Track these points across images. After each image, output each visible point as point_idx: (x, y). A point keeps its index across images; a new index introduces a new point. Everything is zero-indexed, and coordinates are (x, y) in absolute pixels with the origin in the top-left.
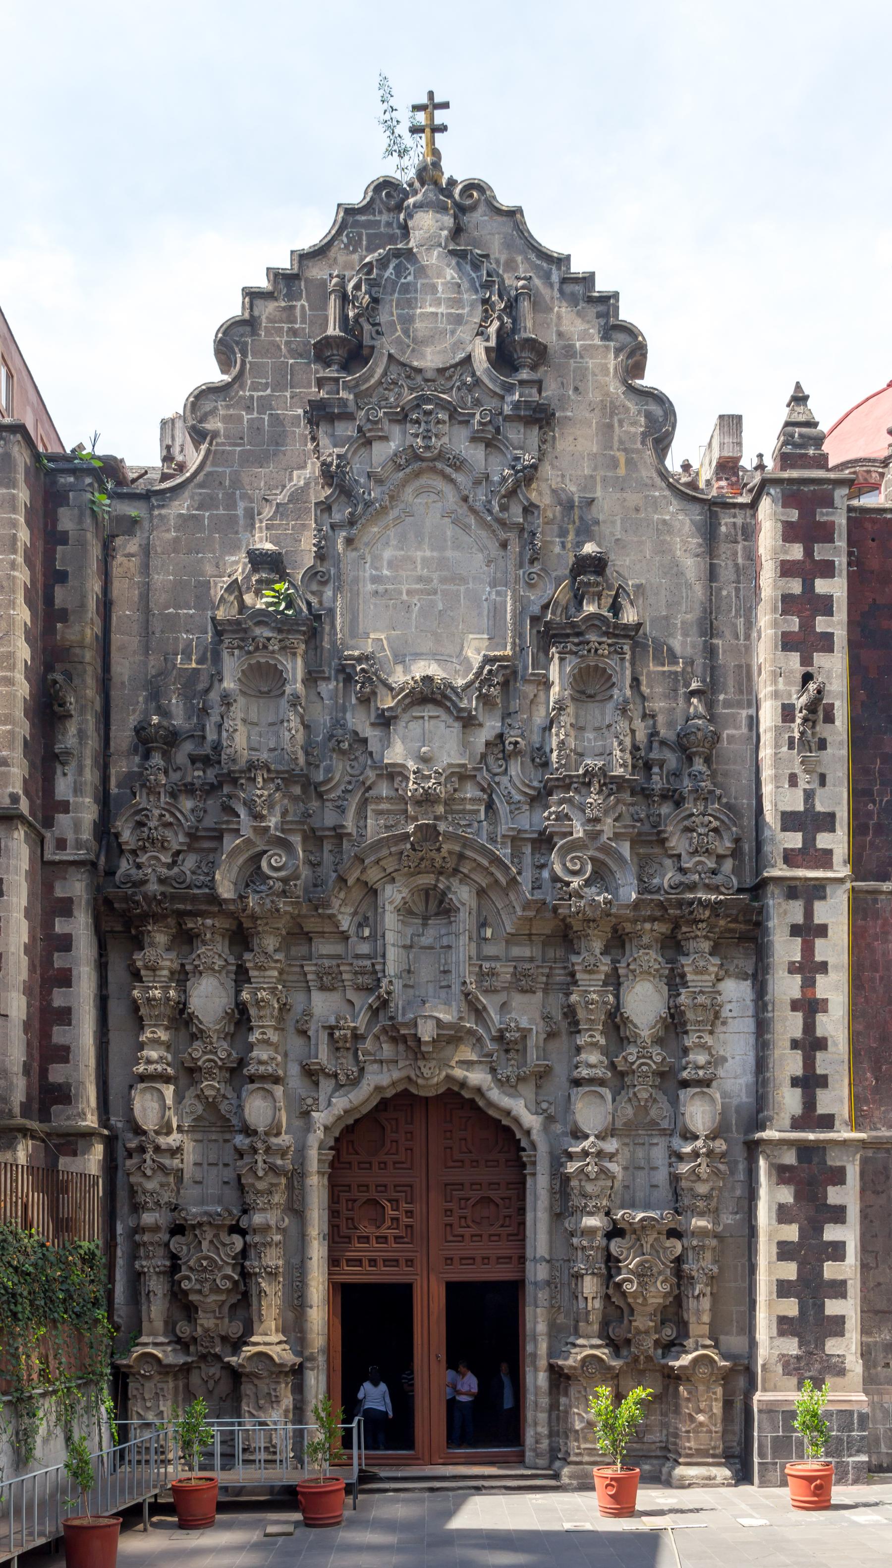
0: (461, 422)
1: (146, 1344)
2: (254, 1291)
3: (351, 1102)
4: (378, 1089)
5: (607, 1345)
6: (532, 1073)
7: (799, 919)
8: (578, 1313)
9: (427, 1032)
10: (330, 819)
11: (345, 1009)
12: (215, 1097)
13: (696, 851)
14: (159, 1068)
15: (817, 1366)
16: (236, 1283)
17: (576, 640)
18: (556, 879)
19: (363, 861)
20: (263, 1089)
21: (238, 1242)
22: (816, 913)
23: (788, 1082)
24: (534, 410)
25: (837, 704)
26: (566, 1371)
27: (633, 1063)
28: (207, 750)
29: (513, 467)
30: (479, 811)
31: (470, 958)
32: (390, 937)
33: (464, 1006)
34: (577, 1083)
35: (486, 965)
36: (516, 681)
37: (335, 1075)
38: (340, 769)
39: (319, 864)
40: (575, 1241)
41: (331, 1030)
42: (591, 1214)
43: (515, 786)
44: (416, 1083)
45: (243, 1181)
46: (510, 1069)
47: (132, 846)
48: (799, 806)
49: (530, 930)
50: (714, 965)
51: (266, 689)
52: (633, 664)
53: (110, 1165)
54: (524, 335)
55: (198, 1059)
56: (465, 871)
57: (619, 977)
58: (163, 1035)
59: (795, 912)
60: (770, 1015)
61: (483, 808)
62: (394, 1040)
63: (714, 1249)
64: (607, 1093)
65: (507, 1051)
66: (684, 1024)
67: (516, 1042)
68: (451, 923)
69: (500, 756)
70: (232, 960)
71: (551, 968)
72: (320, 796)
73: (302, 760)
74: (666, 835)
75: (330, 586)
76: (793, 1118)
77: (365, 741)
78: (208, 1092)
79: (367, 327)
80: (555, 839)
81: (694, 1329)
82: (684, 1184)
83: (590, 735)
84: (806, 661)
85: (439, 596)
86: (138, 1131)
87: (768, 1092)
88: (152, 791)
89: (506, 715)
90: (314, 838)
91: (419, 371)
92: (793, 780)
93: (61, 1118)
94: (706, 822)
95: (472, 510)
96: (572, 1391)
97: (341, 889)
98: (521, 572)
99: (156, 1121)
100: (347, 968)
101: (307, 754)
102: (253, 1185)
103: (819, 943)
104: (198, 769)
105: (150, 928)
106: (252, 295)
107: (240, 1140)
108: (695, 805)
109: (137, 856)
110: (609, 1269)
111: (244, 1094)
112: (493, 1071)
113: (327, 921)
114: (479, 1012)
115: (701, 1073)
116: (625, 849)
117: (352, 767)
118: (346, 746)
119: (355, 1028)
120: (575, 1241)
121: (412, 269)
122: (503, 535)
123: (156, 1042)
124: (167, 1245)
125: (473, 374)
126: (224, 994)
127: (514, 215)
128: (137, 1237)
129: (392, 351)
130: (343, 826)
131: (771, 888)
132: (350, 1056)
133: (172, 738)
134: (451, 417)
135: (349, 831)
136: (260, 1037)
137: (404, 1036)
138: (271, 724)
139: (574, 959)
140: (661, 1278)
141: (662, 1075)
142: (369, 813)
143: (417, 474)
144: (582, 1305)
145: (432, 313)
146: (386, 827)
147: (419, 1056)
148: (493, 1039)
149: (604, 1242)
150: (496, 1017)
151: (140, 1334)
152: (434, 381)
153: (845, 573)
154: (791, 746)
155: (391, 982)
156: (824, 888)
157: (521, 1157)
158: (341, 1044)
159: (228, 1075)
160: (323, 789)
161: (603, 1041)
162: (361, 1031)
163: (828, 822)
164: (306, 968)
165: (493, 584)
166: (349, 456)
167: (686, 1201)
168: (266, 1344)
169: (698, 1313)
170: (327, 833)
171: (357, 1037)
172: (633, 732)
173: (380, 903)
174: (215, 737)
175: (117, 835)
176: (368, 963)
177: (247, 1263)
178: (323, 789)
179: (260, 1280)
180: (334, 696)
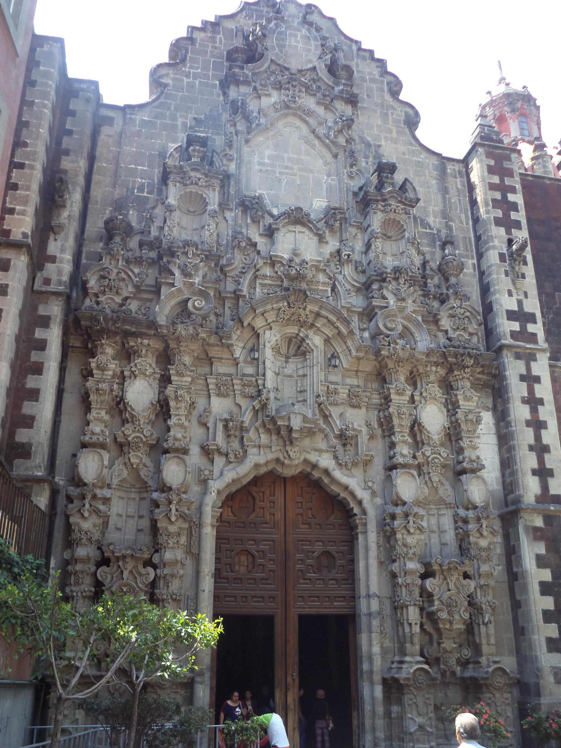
0: (311, 95)
3: (237, 473)
4: (257, 466)
7: (524, 372)
8: (404, 637)
9: (296, 423)
11: (235, 410)
13: (458, 328)
17: (383, 204)
20: (178, 457)
22: (532, 369)
23: (530, 472)
26: (402, 682)
27: (429, 457)
28: (152, 239)
30: (327, 291)
32: (268, 364)
33: (317, 412)
35: (332, 387)
37: (227, 455)
38: (238, 259)
41: (226, 422)
42: (411, 559)
44: (283, 464)
45: (159, 525)
46: (347, 457)
47: (95, 291)
48: (516, 308)
49: (358, 367)
50: (475, 396)
51: (193, 210)
55: (129, 436)
56: (319, 325)
59: (519, 367)
60: (514, 429)
61: (329, 289)
62: (269, 431)
64: (415, 473)
65: (344, 445)
68: (306, 360)
69: (338, 263)
74: (439, 317)
75: (234, 162)
76: (536, 496)
77: (255, 245)
78: (133, 460)
79: (259, 46)
80: (376, 310)
81: (485, 649)
84: (508, 232)
85: (297, 177)
87: (517, 479)
91: (287, 69)
92: (510, 294)
94: (462, 312)
95: (318, 137)
96: (407, 698)
97: (238, 329)
99: (94, 476)
100: (238, 382)
102: (166, 528)
103: (536, 386)
104: (145, 250)
105: (103, 341)
108: (455, 303)
109: (98, 297)
111: (163, 461)
112: (336, 457)
113: (226, 350)
114: (326, 417)
115: (475, 464)
117: (246, 259)
123: (100, 420)
124: (95, 575)
125: (317, 74)
126: (151, 392)
129: (273, 58)
130: (241, 290)
131: (505, 352)
133: (129, 231)
135: (244, 294)
136: (177, 422)
137: (279, 426)
141: (444, 466)
142: (258, 285)
143: (286, 116)
144: (407, 630)
145: (295, 46)
146: (268, 294)
147: (287, 443)
150: (338, 422)
154: (507, 274)
158: (232, 432)
160: (227, 269)
163: (532, 318)
165: (329, 175)
166: (248, 101)
169: (488, 635)
170: (228, 295)
171: (242, 429)
176: (254, 379)
177: (157, 591)
178: (227, 269)
179: (166, 605)
180: (235, 219)
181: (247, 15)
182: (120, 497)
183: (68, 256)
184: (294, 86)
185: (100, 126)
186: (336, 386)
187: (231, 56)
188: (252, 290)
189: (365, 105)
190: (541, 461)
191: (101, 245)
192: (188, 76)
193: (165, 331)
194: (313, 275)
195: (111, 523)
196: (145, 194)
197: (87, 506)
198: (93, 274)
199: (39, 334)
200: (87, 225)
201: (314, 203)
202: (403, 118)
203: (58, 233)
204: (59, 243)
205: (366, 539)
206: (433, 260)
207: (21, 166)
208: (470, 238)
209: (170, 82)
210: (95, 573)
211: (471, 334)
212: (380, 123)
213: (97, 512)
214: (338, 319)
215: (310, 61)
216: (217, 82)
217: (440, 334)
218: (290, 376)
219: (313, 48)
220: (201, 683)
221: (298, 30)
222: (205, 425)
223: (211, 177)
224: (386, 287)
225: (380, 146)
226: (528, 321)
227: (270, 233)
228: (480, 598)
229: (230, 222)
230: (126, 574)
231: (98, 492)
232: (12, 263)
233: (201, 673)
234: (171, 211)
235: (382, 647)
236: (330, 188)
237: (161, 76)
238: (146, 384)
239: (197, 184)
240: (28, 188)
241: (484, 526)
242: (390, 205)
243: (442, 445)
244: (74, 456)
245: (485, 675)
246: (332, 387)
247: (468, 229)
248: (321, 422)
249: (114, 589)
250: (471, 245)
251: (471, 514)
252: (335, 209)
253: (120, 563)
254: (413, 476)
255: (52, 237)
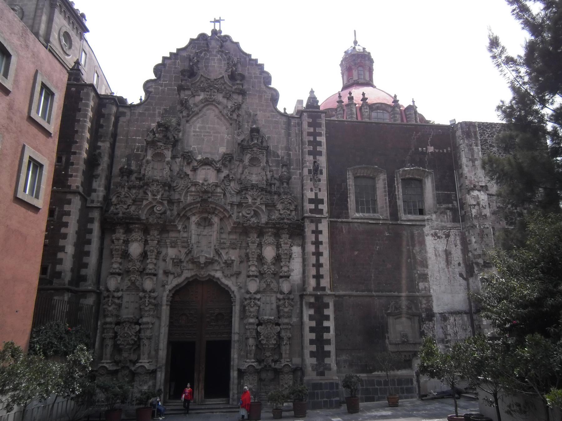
1: (103, 363)
2: (142, 344)
4: (187, 278)
5: (257, 362)
6: (235, 274)
7: (314, 229)
9: (202, 260)
10: (176, 197)
12: (135, 280)
14: (117, 271)
15: (322, 368)
16: (135, 342)
18: (243, 216)
19: (185, 209)
21: (138, 327)
24: (241, 91)
25: (323, 169)
28: (141, 176)
29: (234, 105)
30: (221, 196)
31: (217, 238)
32: (193, 232)
34: (249, 276)
36: (233, 160)
39: (173, 210)
40: (247, 327)
42: (252, 318)
43: (232, 189)
47: (115, 203)
48: (314, 197)
51: (160, 160)
52: (267, 156)
53: (98, 303)
54: (238, 72)
56: (217, 213)
57: (262, 245)
58: (119, 260)
59: (313, 227)
61: (222, 195)
63: (290, 329)
65: (228, 267)
66: (281, 259)
67: (230, 264)
70: (143, 238)
71: (242, 242)
72: (174, 190)
73: (169, 179)
76: (313, 288)
77: (188, 175)
79: (195, 67)
81: (284, 355)
82: (281, 308)
83: (254, 176)
85: (212, 137)
86: (108, 290)
88: (123, 187)
89: (230, 170)
90: (171, 202)
91: (209, 79)
92: (312, 190)
93: (83, 286)
95: (223, 115)
96: (245, 377)
97: (178, 217)
98: (236, 132)
101: (171, 178)
102: (144, 308)
103: (320, 236)
106: (164, 58)
107: (141, 294)
110: (257, 336)
111: (144, 279)
112: (223, 273)
114: (219, 255)
115: (286, 274)
116: (264, 207)
118: (183, 176)
119: (181, 259)
120: (247, 327)
121: (208, 55)
122: (231, 122)
127: (237, 44)
128: (104, 326)
130: (181, 199)
131: (306, 219)
132: (179, 268)
133: (130, 172)
134: (218, 91)
138: (161, 169)
139: (248, 239)
140: (273, 339)
142: (188, 195)
143: (207, 105)
144: (249, 348)
146: (194, 200)
148: (224, 263)
149: (256, 327)
151: (102, 360)
152: (213, 82)
153: (325, 135)
154: (311, 181)
155: (192, 245)
156: (321, 220)
157: (231, 300)
159: (139, 273)
161: (256, 264)
162: (183, 260)
163: (322, 201)
164: (167, 241)
165: (228, 135)
167: (281, 314)
168: (144, 363)
171: (181, 261)
172: (266, 175)
173: (191, 222)
174: (144, 173)
175: (111, 199)
176: (186, 239)
177: (140, 335)
181: (193, 47)
182: (128, 294)
183: (102, 189)
184: (212, 90)
185: (119, 117)
186: (224, 240)
187: (183, 72)
188: (186, 198)
189: (250, 92)
190: (318, 271)
191: (120, 178)
192: (162, 86)
193: (144, 222)
194: (214, 190)
195: (123, 306)
196: (139, 153)
197: (110, 301)
198: (114, 195)
199: (89, 226)
200: (114, 169)
201: (220, 150)
202: (269, 97)
203: (97, 178)
204: (98, 183)
205: (235, 308)
206: (277, 174)
207: (75, 153)
208: (300, 159)
209: (153, 90)
210: (114, 328)
211: (291, 211)
212: (257, 102)
213: (113, 303)
214: (224, 210)
215: (221, 73)
216: (176, 88)
217: (276, 212)
218: (206, 235)
219: (223, 65)
220: (160, 371)
221: (216, 56)
222: (164, 260)
223: (168, 144)
224: (248, 194)
225: (256, 114)
226: (320, 204)
227: (194, 170)
228: (283, 334)
229: (178, 164)
230: (126, 329)
231: (116, 294)
232: (72, 201)
233: (160, 367)
234: (148, 163)
235: (239, 355)
236: (228, 141)
237: (148, 88)
238: (138, 244)
239: (160, 148)
240: (78, 164)
241: (287, 303)
242: (254, 150)
243: (274, 264)
244: (108, 276)
245: (280, 367)
246: (222, 241)
247: (299, 155)
248: (217, 258)
249: (121, 335)
250: (300, 163)
251: (281, 297)
252: (227, 154)
253: (124, 324)
254: (256, 281)
255: (94, 180)
